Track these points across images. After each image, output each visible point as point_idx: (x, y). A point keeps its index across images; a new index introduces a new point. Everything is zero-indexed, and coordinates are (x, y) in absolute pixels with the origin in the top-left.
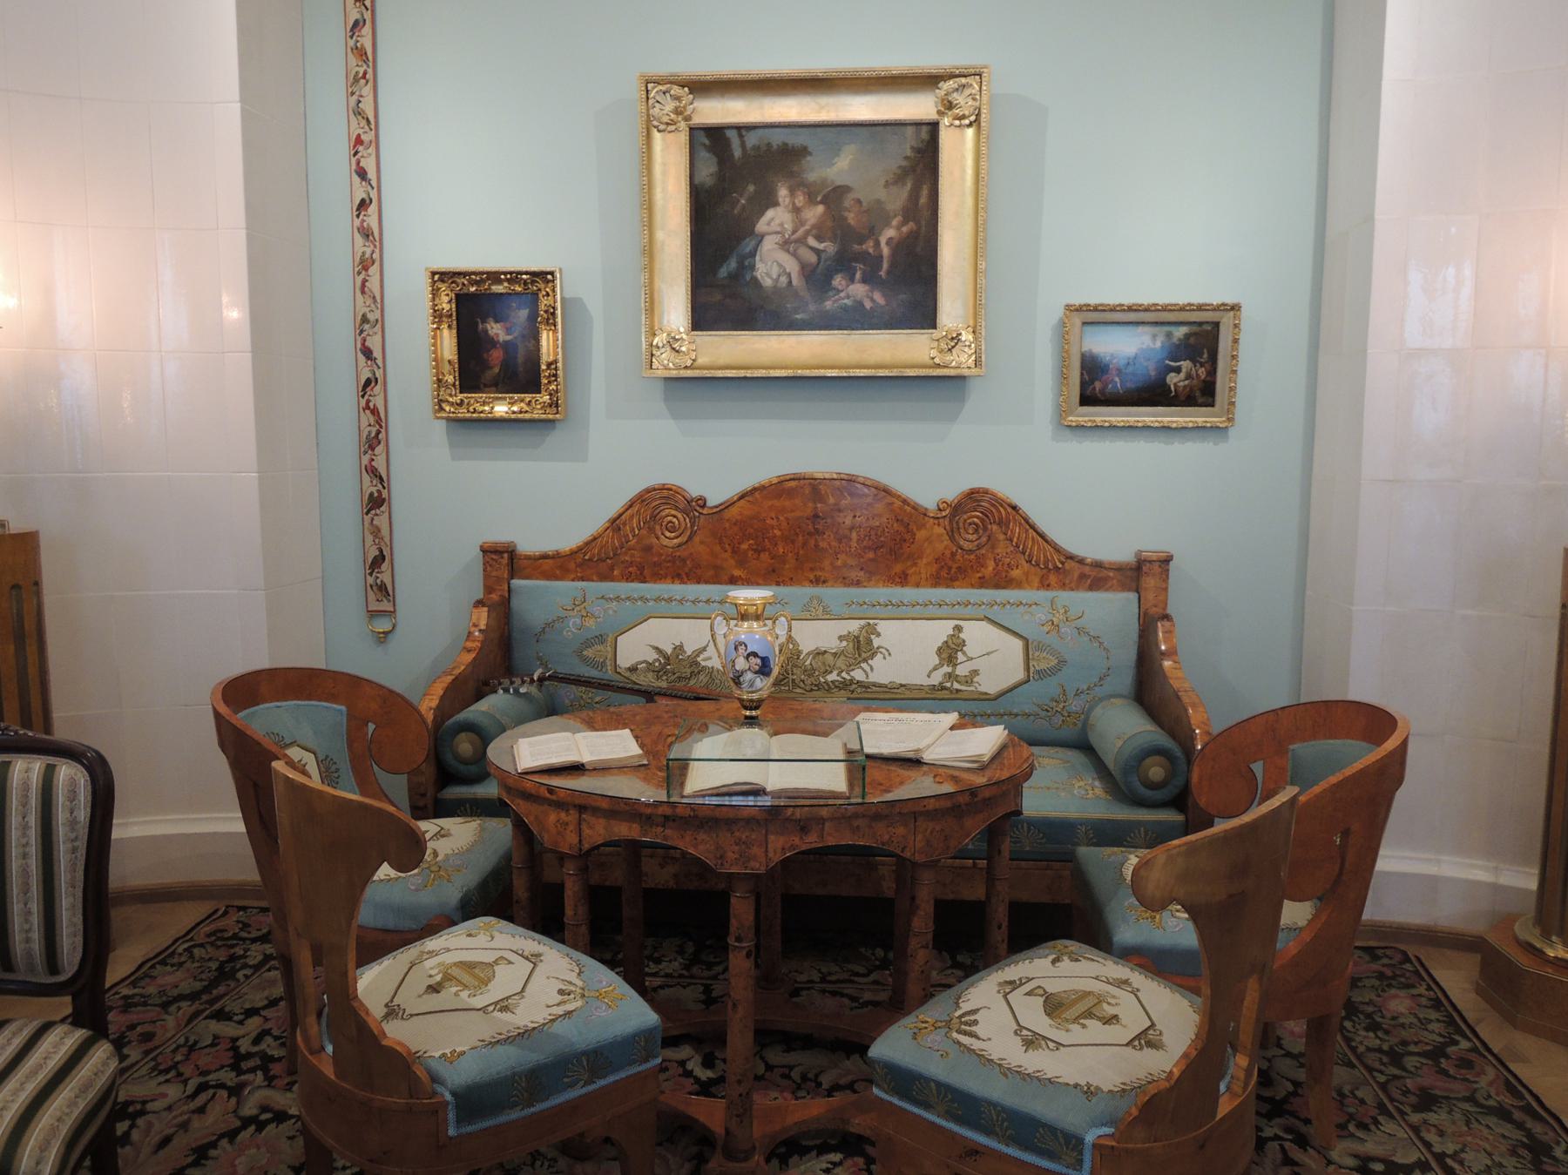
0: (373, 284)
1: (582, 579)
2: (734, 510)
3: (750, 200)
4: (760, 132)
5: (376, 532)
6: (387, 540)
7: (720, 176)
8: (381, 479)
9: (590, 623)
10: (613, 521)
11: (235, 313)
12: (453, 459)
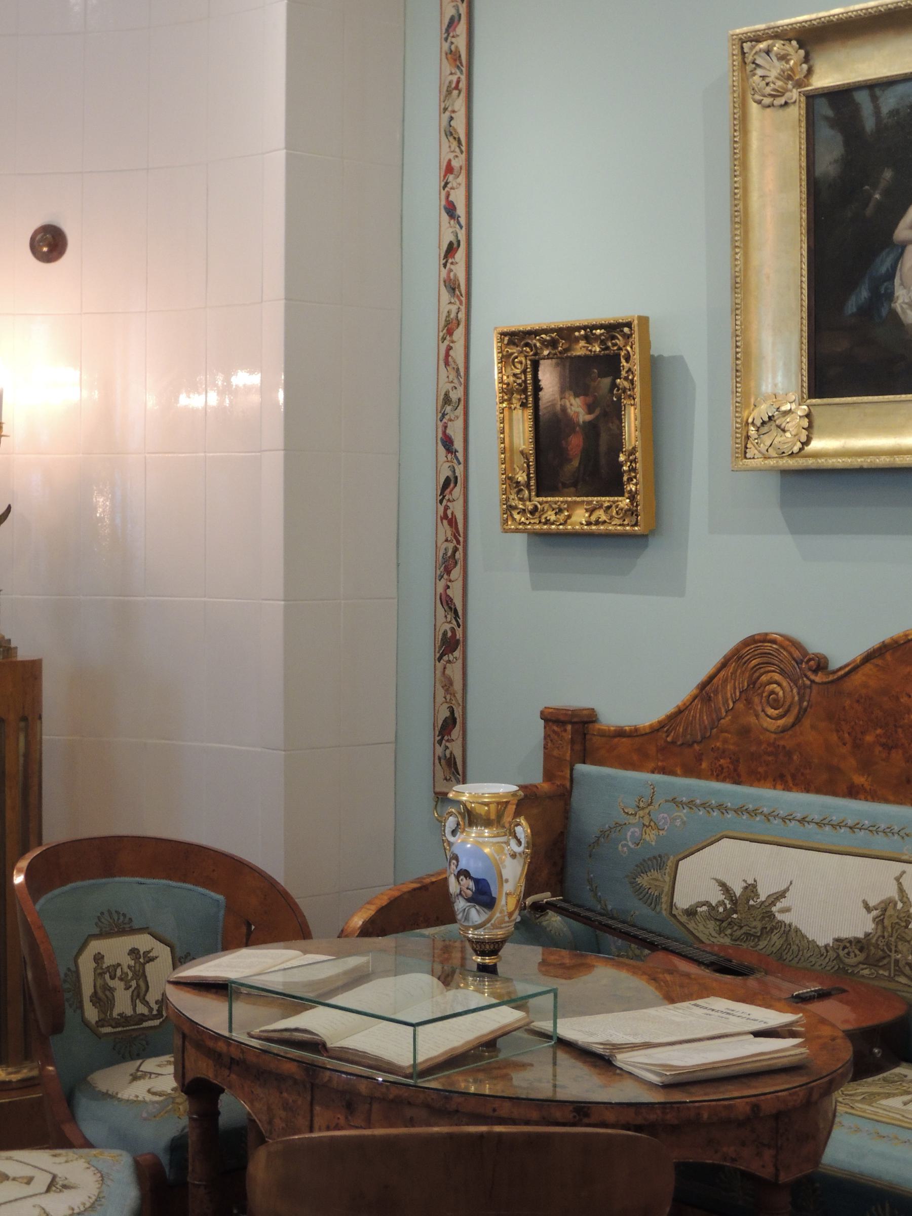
1: (663, 771)
2: (858, 678)
3: (887, 193)
4: (900, 89)
5: (448, 685)
6: (459, 696)
7: (848, 162)
8: (456, 612)
9: (651, 837)
10: (703, 686)
12: (535, 587)
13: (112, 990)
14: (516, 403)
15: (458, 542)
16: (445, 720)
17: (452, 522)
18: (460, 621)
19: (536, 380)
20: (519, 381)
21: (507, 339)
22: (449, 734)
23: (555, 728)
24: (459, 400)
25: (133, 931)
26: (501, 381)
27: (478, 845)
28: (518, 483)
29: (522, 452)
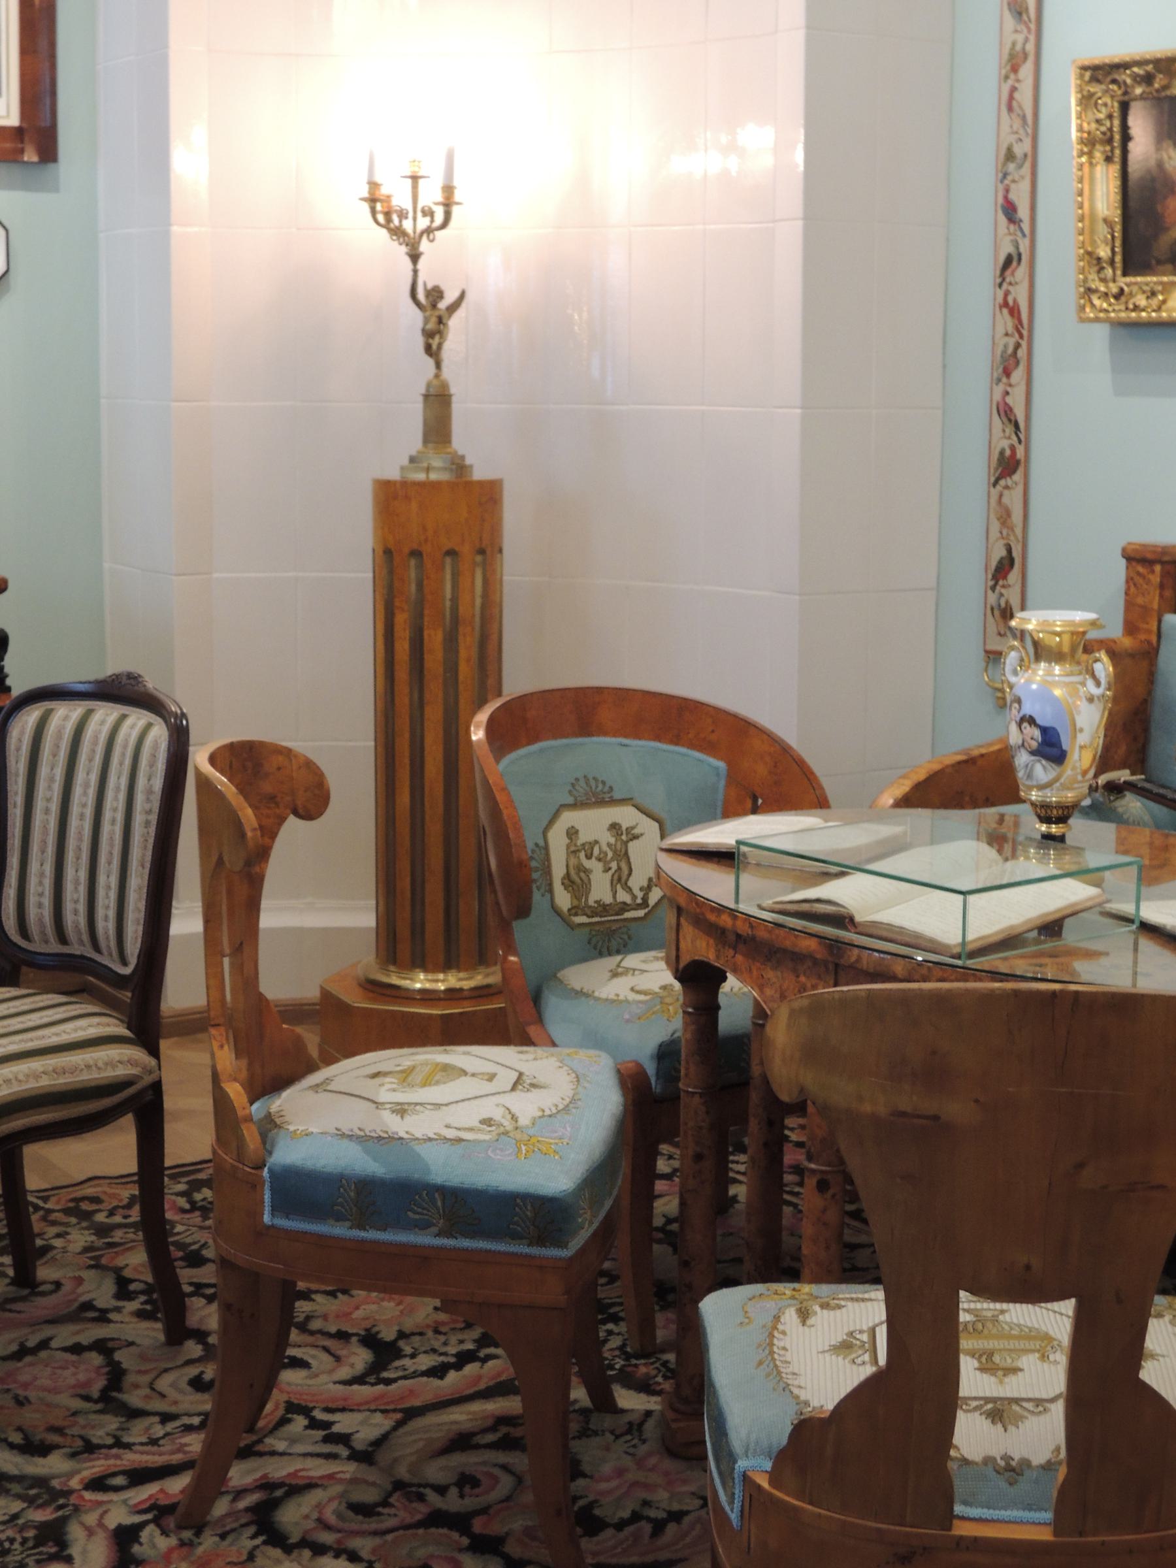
0: (1024, 97)
5: (1005, 517)
6: (1018, 530)
11: (799, 156)
13: (587, 872)
14: (1098, 155)
15: (1021, 336)
16: (1001, 562)
17: (1014, 311)
18: (1022, 436)
19: (1125, 127)
20: (1103, 129)
21: (1088, 75)
22: (1005, 577)
23: (1140, 569)
24: (1026, 155)
25: (613, 802)
26: (1080, 129)
27: (1046, 685)
28: (1099, 259)
29: (1105, 221)
